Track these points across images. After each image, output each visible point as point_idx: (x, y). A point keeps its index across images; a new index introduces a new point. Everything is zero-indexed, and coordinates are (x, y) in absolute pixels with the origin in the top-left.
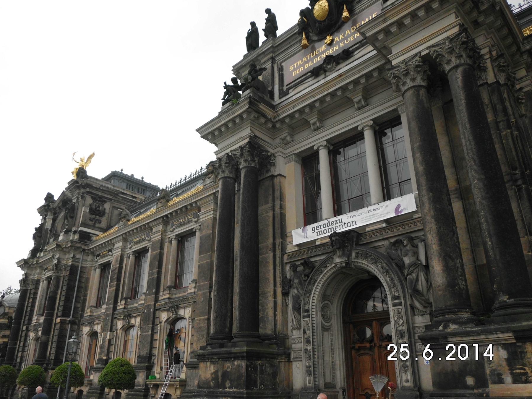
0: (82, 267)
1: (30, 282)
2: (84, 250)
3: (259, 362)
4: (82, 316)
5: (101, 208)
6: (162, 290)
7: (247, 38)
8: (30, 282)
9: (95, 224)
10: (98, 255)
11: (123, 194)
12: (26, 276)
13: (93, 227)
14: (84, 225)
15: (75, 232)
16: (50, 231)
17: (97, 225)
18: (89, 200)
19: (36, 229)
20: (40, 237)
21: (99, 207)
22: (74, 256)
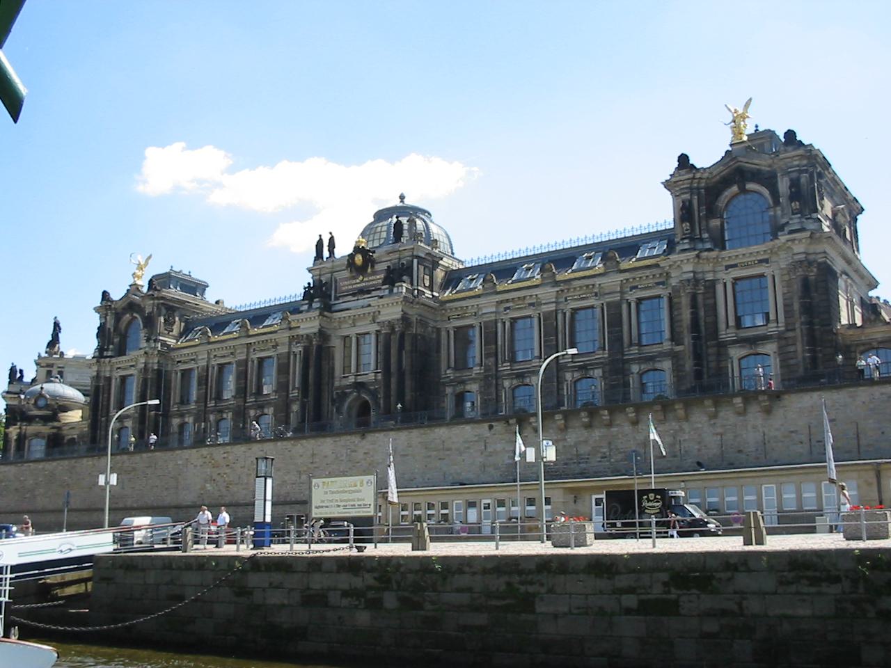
0: (165, 371)
6: (248, 395)
11: (188, 302)
17: (171, 333)
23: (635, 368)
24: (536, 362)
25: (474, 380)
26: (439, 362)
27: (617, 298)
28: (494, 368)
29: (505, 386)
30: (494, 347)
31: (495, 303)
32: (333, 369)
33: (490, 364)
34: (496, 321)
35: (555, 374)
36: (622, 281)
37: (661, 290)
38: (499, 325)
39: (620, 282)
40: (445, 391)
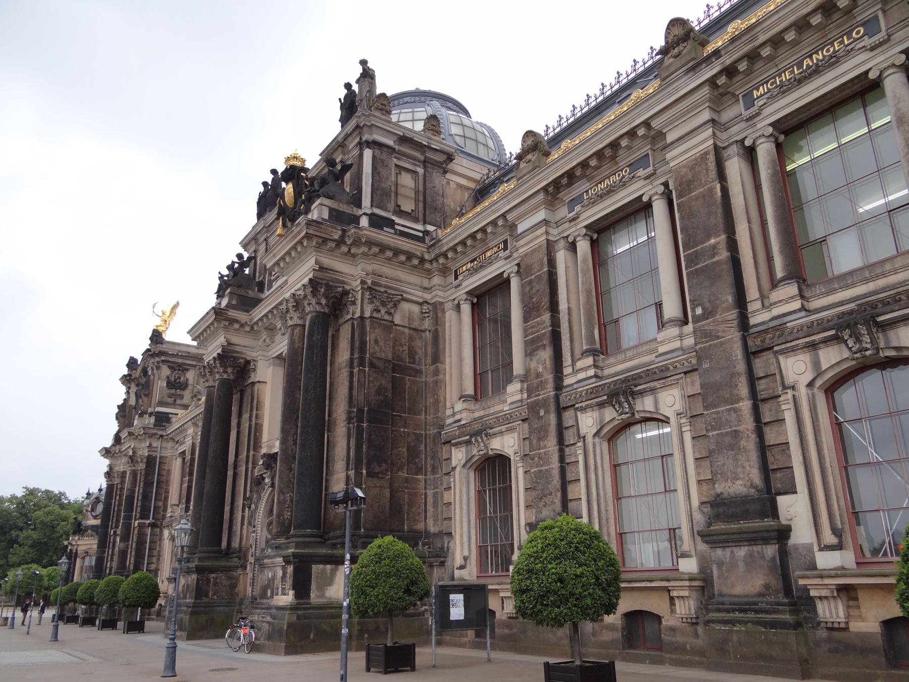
0: (161, 457)
1: (116, 475)
2: (162, 436)
3: (214, 575)
4: (164, 517)
5: (182, 379)
7: (258, 203)
8: (116, 475)
9: (175, 401)
10: (177, 442)
12: (111, 467)
13: (174, 405)
14: (161, 403)
15: (151, 414)
16: (135, 408)
18: (166, 371)
19: (118, 406)
20: (124, 417)
21: (179, 378)
22: (150, 444)
24: (670, 340)
26: (438, 384)
28: (549, 377)
29: (583, 431)
30: (546, 317)
31: (541, 196)
32: (258, 428)
34: (550, 247)
35: (741, 367)
40: (449, 459)
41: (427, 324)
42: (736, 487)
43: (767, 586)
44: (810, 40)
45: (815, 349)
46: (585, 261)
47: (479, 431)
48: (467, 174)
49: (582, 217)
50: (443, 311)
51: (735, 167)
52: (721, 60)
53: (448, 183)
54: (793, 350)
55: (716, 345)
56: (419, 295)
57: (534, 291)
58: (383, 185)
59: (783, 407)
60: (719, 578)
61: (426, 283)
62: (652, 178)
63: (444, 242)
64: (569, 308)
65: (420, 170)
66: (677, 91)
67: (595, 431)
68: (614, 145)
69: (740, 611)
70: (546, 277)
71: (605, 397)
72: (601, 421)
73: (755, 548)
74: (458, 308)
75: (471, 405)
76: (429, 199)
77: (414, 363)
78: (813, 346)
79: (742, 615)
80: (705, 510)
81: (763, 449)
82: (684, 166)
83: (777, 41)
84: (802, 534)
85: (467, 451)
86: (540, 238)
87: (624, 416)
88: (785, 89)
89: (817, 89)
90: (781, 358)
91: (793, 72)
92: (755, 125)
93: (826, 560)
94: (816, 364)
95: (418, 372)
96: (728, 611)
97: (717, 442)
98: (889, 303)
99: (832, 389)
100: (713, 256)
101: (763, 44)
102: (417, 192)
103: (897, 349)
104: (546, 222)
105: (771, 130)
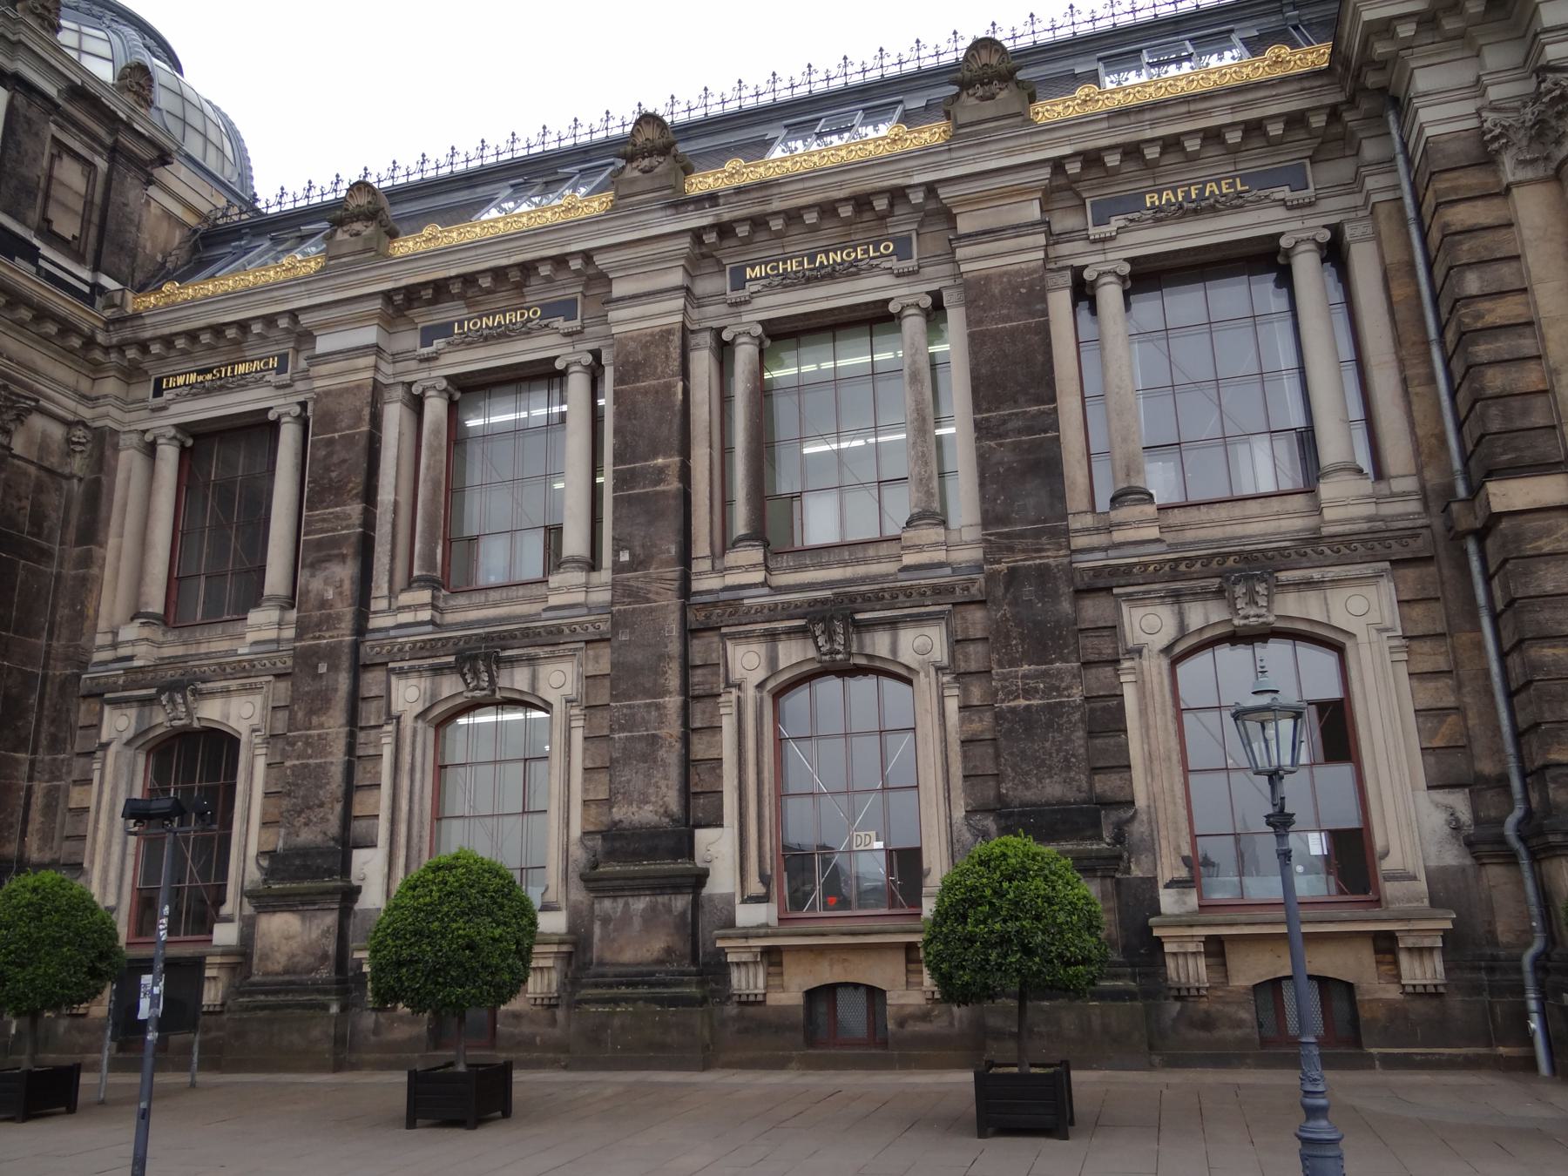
23: (1149, 624)
24: (570, 589)
25: (241, 673)
26: (85, 585)
27: (1026, 254)
28: (347, 611)
29: (397, 707)
30: (355, 509)
33: (330, 594)
34: (377, 392)
35: (674, 648)
36: (1058, 164)
37: (1280, 212)
38: (394, 415)
39: (1045, 173)
40: (97, 726)
41: (77, 465)
42: (645, 815)
43: (669, 951)
44: (831, 232)
45: (774, 641)
46: (436, 432)
47: (183, 683)
48: (180, 196)
49: (445, 360)
50: (116, 449)
51: (703, 363)
52: (716, 210)
53: (148, 203)
54: (747, 636)
55: (644, 610)
56: (68, 406)
57: (335, 459)
58: (24, 171)
59: (722, 711)
60: (602, 940)
61: (85, 385)
62: (575, 338)
63: (148, 321)
64: (396, 503)
65: (102, 164)
66: (645, 226)
67: (419, 708)
68: (528, 268)
69: (628, 985)
70: (363, 442)
71: (452, 659)
72: (433, 695)
73: (660, 899)
74: (151, 450)
75: (157, 633)
76: (111, 225)
77: (38, 535)
78: (772, 636)
79: (630, 990)
80: (590, 844)
81: (687, 763)
82: (631, 338)
83: (793, 216)
84: (723, 881)
85: (140, 718)
86: (362, 372)
87: (478, 693)
88: (788, 282)
89: (827, 298)
90: (729, 644)
91: (801, 264)
92: (739, 314)
93: (748, 915)
94: (773, 660)
95: (45, 555)
96: (610, 986)
97: (625, 749)
98: (869, 599)
99: (779, 694)
100: (658, 483)
101: (776, 214)
102: (88, 203)
103: (870, 657)
104: (377, 349)
105: (759, 330)
